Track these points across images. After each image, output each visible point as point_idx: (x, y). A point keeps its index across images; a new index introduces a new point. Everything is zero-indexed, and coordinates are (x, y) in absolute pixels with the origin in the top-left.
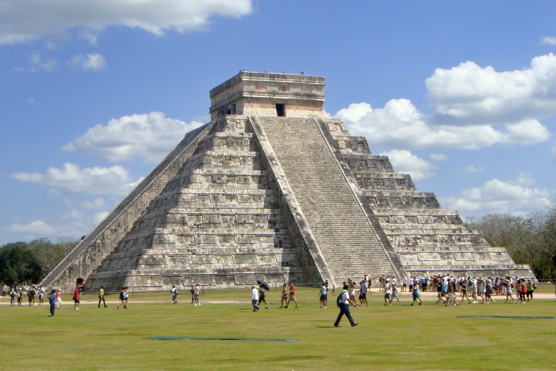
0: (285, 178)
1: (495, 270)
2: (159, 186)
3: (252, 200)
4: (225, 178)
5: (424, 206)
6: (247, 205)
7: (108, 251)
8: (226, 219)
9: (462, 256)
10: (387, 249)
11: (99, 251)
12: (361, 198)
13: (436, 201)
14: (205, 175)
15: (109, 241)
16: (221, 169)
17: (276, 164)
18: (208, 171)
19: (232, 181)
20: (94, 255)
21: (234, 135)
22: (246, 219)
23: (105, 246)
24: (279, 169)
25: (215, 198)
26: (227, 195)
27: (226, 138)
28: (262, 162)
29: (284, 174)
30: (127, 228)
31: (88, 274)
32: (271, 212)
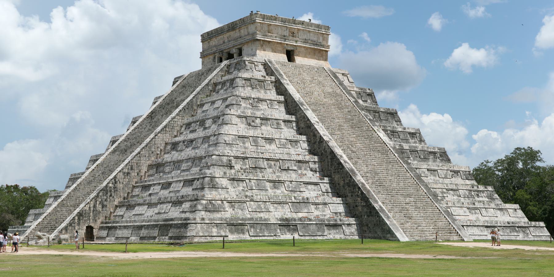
0: (321, 124)
1: (518, 227)
4: (258, 121)
7: (120, 197)
8: (271, 165)
9: (487, 212)
11: (111, 196)
14: (239, 117)
15: (121, 185)
17: (308, 109)
19: (265, 124)
20: (106, 200)
22: (290, 165)
23: (117, 191)
26: (266, 139)
28: (292, 107)
29: (318, 120)
31: (99, 221)
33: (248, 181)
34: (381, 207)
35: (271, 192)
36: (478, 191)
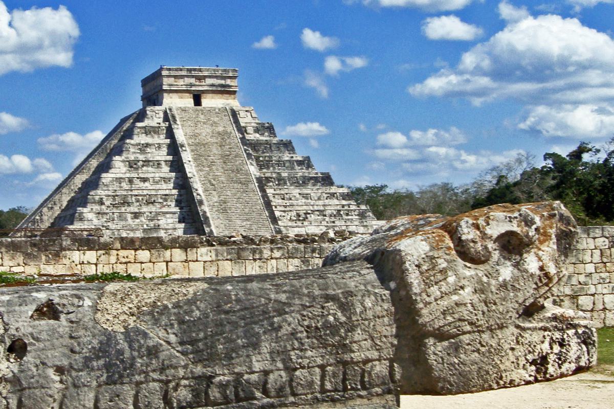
2: (90, 169)
3: (163, 182)
4: (140, 163)
5: (319, 184)
6: (158, 187)
10: (273, 224)
12: (257, 179)
13: (331, 179)
14: (123, 161)
16: (138, 155)
17: (185, 150)
18: (126, 158)
21: (151, 125)
22: (156, 199)
24: (188, 154)
25: (131, 181)
26: (141, 178)
27: (144, 127)
28: (174, 148)
30: (62, 205)
32: (178, 192)
33: (111, 214)
34: (211, 231)
35: (130, 221)
36: (348, 210)
